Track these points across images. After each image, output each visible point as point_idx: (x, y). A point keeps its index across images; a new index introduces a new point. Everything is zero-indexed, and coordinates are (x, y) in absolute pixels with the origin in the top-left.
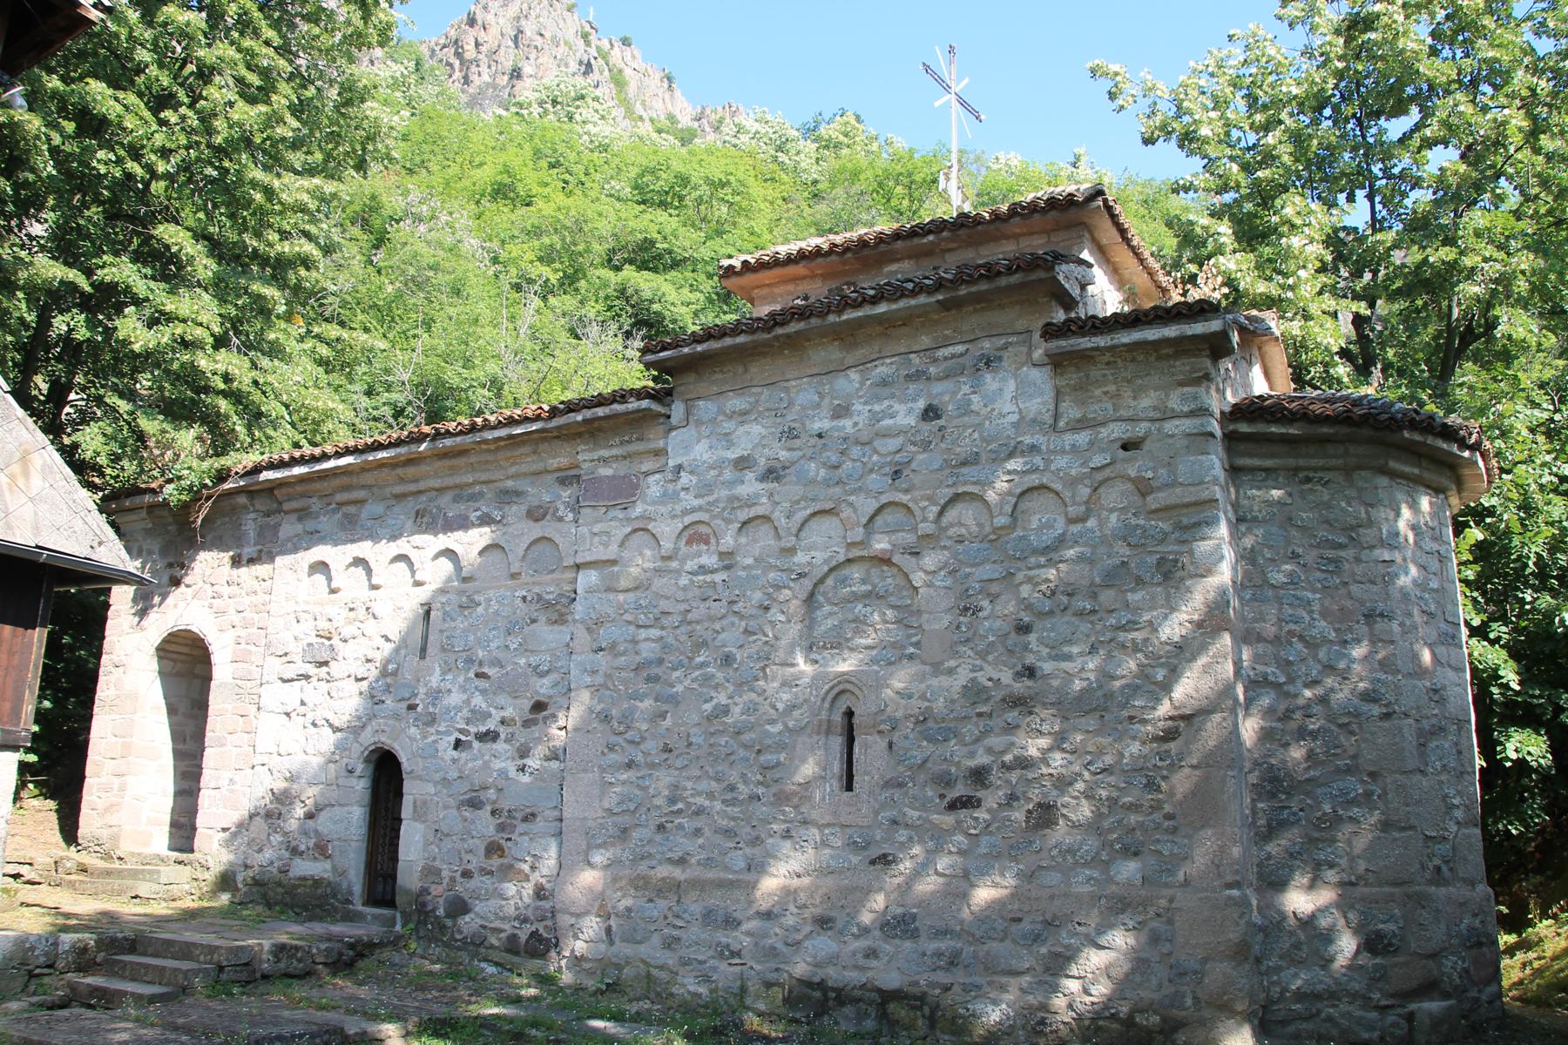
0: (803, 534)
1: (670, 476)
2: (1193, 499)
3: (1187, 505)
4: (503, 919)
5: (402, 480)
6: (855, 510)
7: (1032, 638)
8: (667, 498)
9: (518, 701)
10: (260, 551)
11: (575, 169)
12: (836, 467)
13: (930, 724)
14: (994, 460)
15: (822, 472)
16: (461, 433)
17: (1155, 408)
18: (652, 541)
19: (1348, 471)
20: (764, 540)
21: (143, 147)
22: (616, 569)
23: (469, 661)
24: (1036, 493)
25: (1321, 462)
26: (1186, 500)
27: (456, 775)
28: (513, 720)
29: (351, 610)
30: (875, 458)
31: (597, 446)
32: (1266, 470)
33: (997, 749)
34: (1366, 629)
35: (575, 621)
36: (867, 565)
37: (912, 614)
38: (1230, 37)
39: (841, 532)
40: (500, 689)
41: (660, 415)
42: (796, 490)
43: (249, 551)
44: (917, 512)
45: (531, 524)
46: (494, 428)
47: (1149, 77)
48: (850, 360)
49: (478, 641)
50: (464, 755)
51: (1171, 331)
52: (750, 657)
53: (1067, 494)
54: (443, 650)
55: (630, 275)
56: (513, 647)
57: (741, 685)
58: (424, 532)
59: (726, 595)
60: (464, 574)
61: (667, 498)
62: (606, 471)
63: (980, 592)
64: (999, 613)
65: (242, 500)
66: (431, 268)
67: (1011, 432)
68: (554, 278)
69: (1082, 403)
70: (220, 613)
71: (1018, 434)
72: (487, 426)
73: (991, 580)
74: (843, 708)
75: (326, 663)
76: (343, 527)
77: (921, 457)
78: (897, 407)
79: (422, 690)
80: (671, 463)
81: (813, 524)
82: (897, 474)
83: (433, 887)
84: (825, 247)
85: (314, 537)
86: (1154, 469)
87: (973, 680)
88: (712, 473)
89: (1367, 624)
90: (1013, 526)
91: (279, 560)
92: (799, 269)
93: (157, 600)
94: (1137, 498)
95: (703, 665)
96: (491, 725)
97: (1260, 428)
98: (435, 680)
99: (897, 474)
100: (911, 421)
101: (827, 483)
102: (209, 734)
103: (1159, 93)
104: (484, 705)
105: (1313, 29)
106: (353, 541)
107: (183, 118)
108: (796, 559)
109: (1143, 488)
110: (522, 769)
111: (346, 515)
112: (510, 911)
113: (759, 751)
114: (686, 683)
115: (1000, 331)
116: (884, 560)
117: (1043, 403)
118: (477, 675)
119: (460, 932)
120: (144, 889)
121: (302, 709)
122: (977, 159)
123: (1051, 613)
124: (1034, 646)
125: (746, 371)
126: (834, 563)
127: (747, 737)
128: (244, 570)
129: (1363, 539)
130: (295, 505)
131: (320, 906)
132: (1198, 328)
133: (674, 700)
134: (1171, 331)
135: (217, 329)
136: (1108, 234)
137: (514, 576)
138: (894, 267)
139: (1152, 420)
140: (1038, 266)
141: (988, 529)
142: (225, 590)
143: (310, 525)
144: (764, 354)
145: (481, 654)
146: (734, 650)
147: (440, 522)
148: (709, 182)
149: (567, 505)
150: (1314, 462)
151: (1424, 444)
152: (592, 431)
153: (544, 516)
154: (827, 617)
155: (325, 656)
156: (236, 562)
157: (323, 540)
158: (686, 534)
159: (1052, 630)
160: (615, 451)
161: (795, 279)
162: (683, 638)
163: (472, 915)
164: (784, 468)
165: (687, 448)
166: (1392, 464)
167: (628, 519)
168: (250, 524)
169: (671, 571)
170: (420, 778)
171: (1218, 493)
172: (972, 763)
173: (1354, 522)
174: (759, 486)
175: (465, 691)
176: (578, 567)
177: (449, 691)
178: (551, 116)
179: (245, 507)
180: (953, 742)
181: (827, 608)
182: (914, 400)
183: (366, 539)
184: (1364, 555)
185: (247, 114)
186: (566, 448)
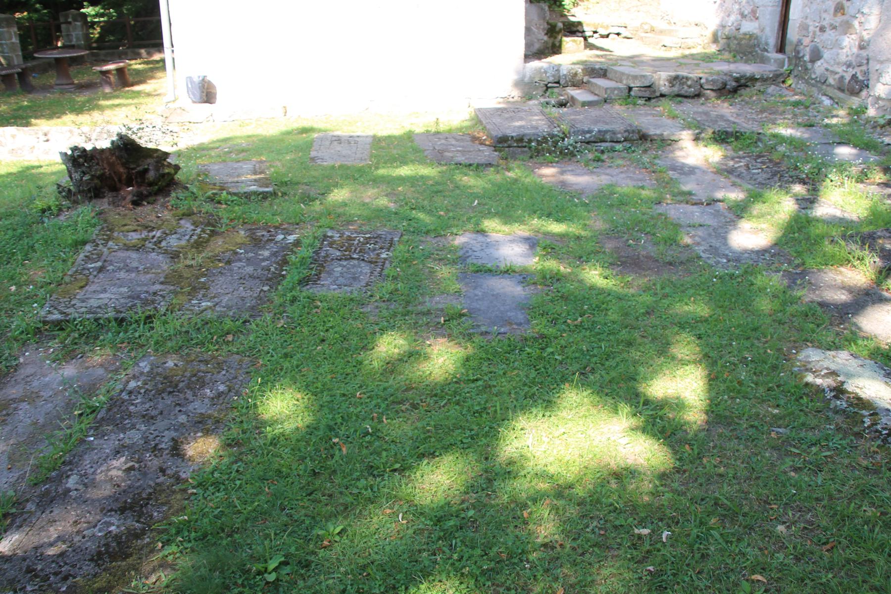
4: (838, 64)
83: (804, 38)
112: (843, 58)
119: (815, 73)
120: (667, 40)
131: (751, 53)
163: (822, 61)
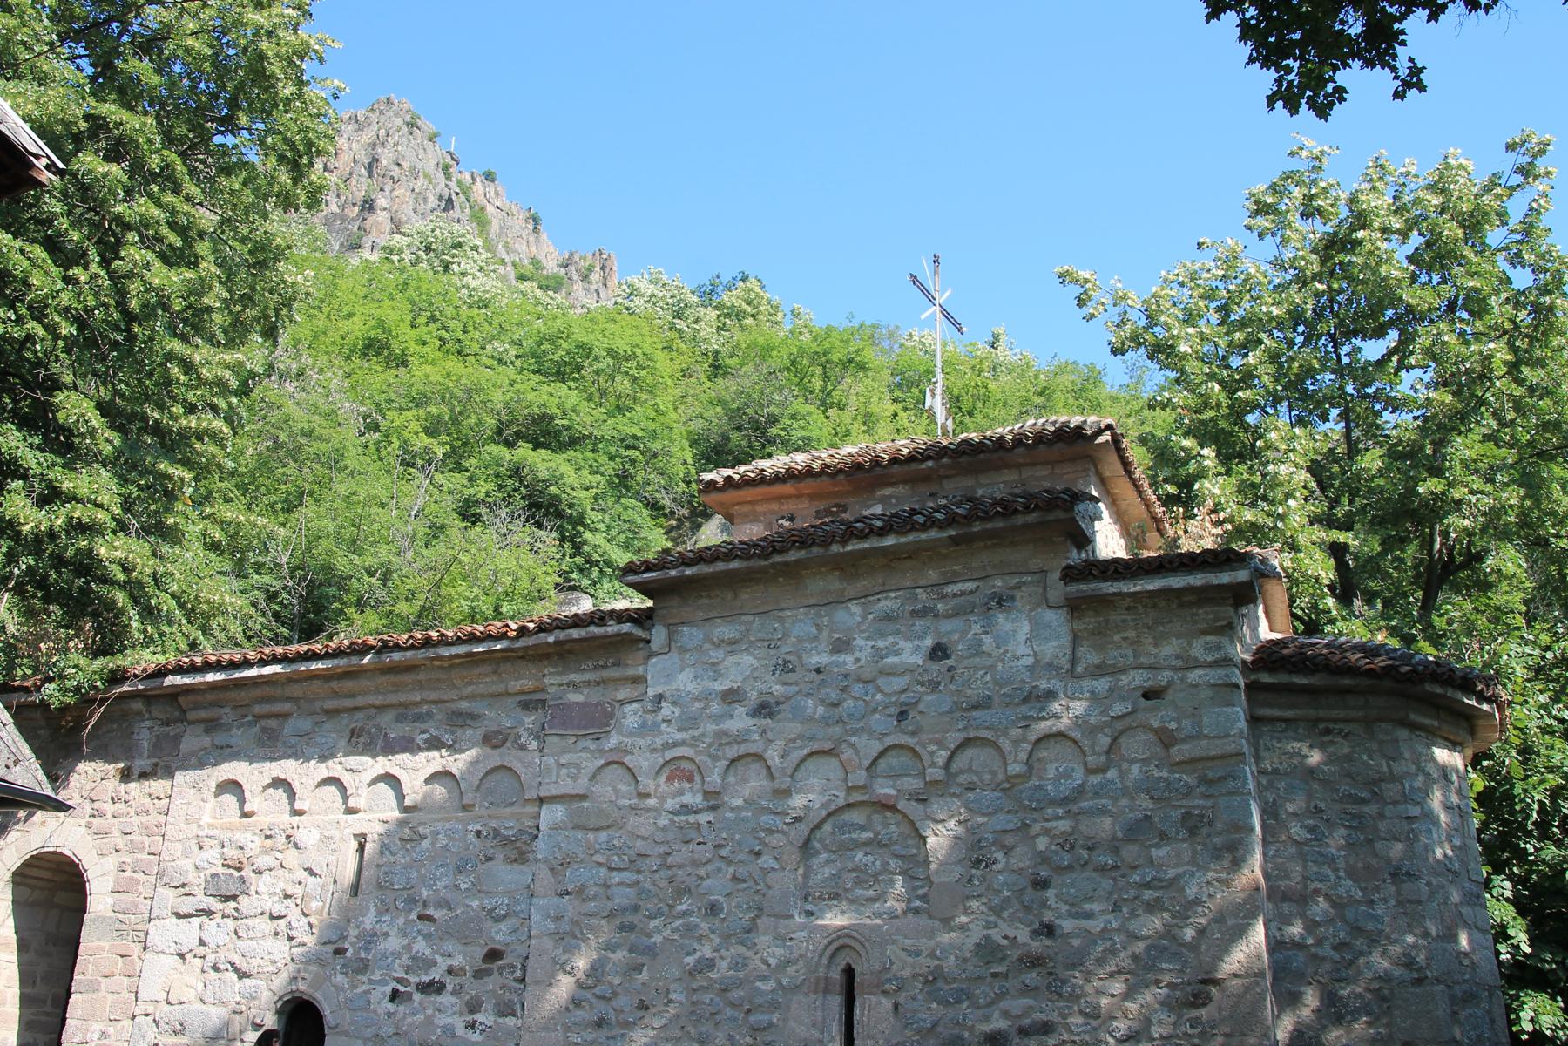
0: (798, 775)
2: (1219, 752)
3: (1214, 758)
5: (336, 694)
6: (857, 752)
7: (1051, 893)
8: (644, 729)
9: (469, 949)
10: (156, 765)
11: (453, 324)
12: (836, 705)
13: (940, 984)
14: (1008, 705)
15: (821, 710)
16: (412, 647)
17: (1178, 657)
18: (628, 777)
20: (753, 783)
22: (586, 804)
23: (411, 901)
24: (1052, 741)
25: (1342, 714)
27: (391, 1031)
28: (462, 969)
29: (267, 837)
30: (879, 697)
32: (1286, 720)
33: (1015, 1012)
34: (1392, 889)
35: (537, 860)
37: (918, 864)
38: (1200, 246)
39: (840, 774)
40: (447, 934)
41: (641, 640)
42: (795, 728)
44: (925, 757)
45: (489, 751)
47: (1119, 285)
48: (851, 591)
49: (422, 879)
50: (401, 1008)
51: (1197, 580)
52: (738, 906)
53: (1086, 743)
55: (524, 451)
56: (463, 887)
58: (362, 753)
59: (711, 837)
60: (408, 802)
61: (644, 729)
62: (575, 697)
63: (993, 844)
64: (1009, 866)
65: (137, 705)
66: (304, 435)
67: (1026, 676)
68: (440, 451)
69: (1100, 648)
70: (100, 834)
72: (444, 641)
73: (1005, 831)
74: (842, 965)
75: (234, 898)
76: (260, 742)
77: (929, 698)
78: (902, 644)
79: (353, 932)
80: (651, 692)
81: (810, 764)
82: (902, 715)
84: (817, 465)
85: (225, 753)
86: (1178, 721)
87: (987, 937)
88: (697, 705)
89: (1393, 883)
90: (1028, 775)
91: (180, 777)
92: (787, 488)
95: (685, 914)
96: (435, 974)
97: (1282, 678)
98: (369, 921)
99: (902, 715)
100: (918, 660)
101: (826, 722)
103: (1130, 302)
104: (428, 952)
105: (1284, 241)
106: (272, 759)
108: (791, 802)
109: (1166, 739)
110: (472, 1026)
111: (264, 730)
113: (749, 1011)
114: (667, 933)
115: (1013, 569)
116: (887, 806)
118: (420, 917)
122: (891, 335)
123: (1070, 868)
124: (1052, 902)
125: (736, 596)
126: (833, 807)
127: (735, 994)
128: (133, 785)
130: (203, 714)
132: (1225, 578)
133: (651, 951)
134: (1197, 580)
137: (465, 808)
138: (887, 491)
139: (1174, 669)
140: (1057, 506)
142: (109, 808)
143: (220, 739)
145: (425, 893)
146: (721, 899)
147: (380, 743)
148: (612, 353)
149: (531, 732)
150: (1334, 713)
151: (1444, 696)
152: (563, 654)
153: (504, 743)
154: (824, 869)
155: (233, 889)
156: (126, 776)
157: (235, 755)
158: (667, 770)
159: (1072, 885)
160: (587, 676)
161: (779, 498)
162: (663, 883)
164: (778, 703)
165: (669, 677)
166: (1413, 717)
167: (601, 751)
168: (144, 734)
169: (648, 810)
170: (346, 1034)
171: (1246, 749)
172: (986, 1028)
173: (1376, 776)
174: (750, 722)
175: (405, 935)
176: (541, 801)
177: (386, 934)
178: (424, 265)
179: (139, 714)
180: (965, 1005)
181: (824, 856)
182: (921, 638)
183: (289, 757)
184: (1389, 810)
185: (162, 276)
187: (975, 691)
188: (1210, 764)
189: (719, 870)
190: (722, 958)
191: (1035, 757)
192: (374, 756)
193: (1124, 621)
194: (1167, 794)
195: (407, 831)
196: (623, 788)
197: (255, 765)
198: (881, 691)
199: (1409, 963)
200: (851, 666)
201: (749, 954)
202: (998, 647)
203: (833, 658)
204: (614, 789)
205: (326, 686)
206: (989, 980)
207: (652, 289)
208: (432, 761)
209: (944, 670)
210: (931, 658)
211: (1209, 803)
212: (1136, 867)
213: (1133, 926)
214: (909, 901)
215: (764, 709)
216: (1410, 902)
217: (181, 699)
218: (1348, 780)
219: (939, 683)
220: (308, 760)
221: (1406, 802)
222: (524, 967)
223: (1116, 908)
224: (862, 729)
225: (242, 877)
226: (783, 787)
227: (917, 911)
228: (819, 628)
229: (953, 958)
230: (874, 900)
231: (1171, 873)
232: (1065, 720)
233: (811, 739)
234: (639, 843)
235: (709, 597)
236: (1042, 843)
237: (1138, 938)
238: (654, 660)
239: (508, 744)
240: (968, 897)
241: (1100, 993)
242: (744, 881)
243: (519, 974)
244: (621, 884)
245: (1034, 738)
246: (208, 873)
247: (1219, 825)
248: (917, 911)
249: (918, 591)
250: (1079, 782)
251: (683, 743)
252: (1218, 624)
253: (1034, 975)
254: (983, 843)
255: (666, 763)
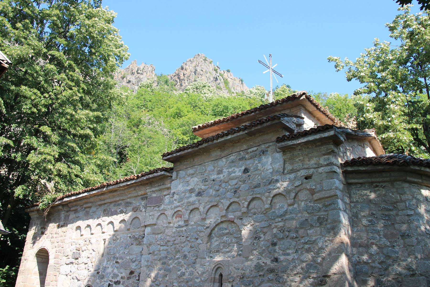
0: (208, 214)
1: (171, 196)
2: (328, 195)
3: (327, 198)
5: (101, 200)
6: (223, 205)
7: (277, 247)
8: (171, 203)
9: (126, 271)
10: (64, 223)
11: (201, 107)
12: (218, 191)
13: (245, 279)
14: (265, 185)
16: (114, 185)
17: (315, 164)
19: (392, 182)
20: (196, 217)
21: (38, 104)
22: (156, 227)
23: (114, 258)
24: (278, 196)
25: (381, 180)
26: (326, 196)
28: (124, 277)
29: (85, 241)
30: (229, 187)
31: (152, 187)
32: (361, 183)
36: (227, 223)
41: (168, 176)
42: (207, 199)
43: (62, 223)
44: (241, 205)
46: (123, 182)
47: (347, 60)
48: (223, 155)
51: (317, 136)
52: (191, 256)
54: (108, 254)
57: (189, 265)
58: (106, 216)
59: (185, 235)
62: (154, 195)
66: (148, 138)
67: (270, 175)
69: (292, 164)
70: (53, 243)
71: (272, 176)
72: (121, 182)
73: (264, 227)
74: (219, 274)
77: (242, 186)
78: (236, 169)
79: (101, 267)
80: (172, 192)
81: (211, 210)
82: (235, 192)
85: (78, 219)
86: (315, 185)
87: (258, 263)
88: (183, 194)
89: (402, 239)
90: (271, 208)
93: (38, 238)
94: (310, 196)
95: (178, 258)
96: (118, 279)
97: (356, 168)
98: (105, 264)
99: (235, 192)
101: (215, 196)
102: (46, 282)
103: (351, 64)
104: (117, 272)
106: (87, 219)
107: (50, 96)
108: (206, 222)
109: (312, 192)
111: (86, 211)
115: (267, 141)
117: (280, 165)
121: (70, 274)
122: (324, 95)
123: (283, 238)
124: (277, 250)
125: (194, 160)
126: (217, 223)
128: (60, 229)
129: (399, 207)
130: (73, 209)
132: (326, 134)
133: (169, 270)
134: (317, 136)
135: (57, 156)
136: (311, 108)
139: (315, 168)
140: (275, 119)
141: (263, 209)
142: (55, 235)
143: (77, 215)
144: (198, 155)
145: (117, 255)
146: (187, 253)
147: (110, 213)
149: (143, 206)
150: (378, 180)
151: (420, 170)
153: (137, 210)
154: (215, 242)
155: (77, 256)
156: (59, 227)
158: (175, 215)
160: (157, 189)
165: (176, 187)
166: (408, 178)
169: (171, 227)
173: (395, 201)
174: (196, 198)
176: (146, 226)
178: (196, 93)
179: (62, 210)
181: (215, 239)
182: (241, 167)
184: (400, 213)
186: (143, 188)
187: (255, 183)
188: (327, 200)
189: (187, 244)
190: (187, 272)
191: (273, 202)
192: (108, 217)
193: (298, 154)
194: (312, 211)
195: (114, 237)
196: (165, 221)
197: (84, 221)
198: (230, 185)
199: (409, 269)
200: (222, 178)
201: (194, 270)
202: (262, 167)
203: (218, 176)
204: (163, 222)
205: (98, 198)
206: (258, 277)
207: (256, 91)
208: (121, 217)
209: (247, 176)
210: (244, 173)
211: (326, 213)
212: (303, 237)
213: (302, 258)
214: (238, 252)
215: (199, 194)
216: (408, 245)
217: (69, 205)
218: (385, 203)
219: (245, 181)
220: (95, 219)
221: (407, 209)
222: (139, 276)
223: (297, 251)
224: (225, 197)
225: (79, 253)
226: (204, 217)
227: (240, 255)
228: (214, 167)
229: (248, 270)
230: (228, 252)
231: (314, 238)
232: (281, 189)
233: (211, 202)
234: (168, 237)
235: (187, 161)
236: (275, 231)
237: (303, 262)
238: (173, 182)
239: (138, 210)
240: (253, 250)
241: (292, 281)
242: (193, 248)
243: (137, 278)
244: (163, 250)
245: (272, 196)
246: (73, 252)
247: (329, 221)
248: (240, 255)
249: (241, 152)
250: (286, 209)
251: (179, 206)
252: (328, 151)
253: (272, 275)
254: (258, 232)
255: (175, 213)
